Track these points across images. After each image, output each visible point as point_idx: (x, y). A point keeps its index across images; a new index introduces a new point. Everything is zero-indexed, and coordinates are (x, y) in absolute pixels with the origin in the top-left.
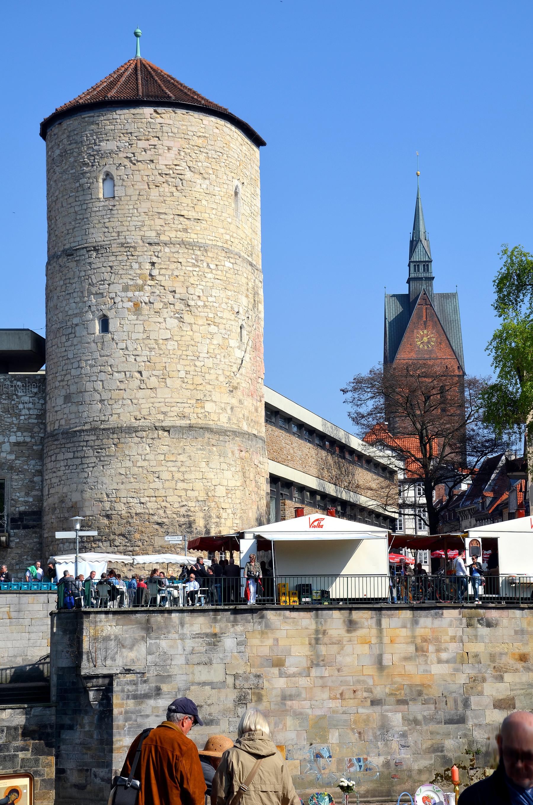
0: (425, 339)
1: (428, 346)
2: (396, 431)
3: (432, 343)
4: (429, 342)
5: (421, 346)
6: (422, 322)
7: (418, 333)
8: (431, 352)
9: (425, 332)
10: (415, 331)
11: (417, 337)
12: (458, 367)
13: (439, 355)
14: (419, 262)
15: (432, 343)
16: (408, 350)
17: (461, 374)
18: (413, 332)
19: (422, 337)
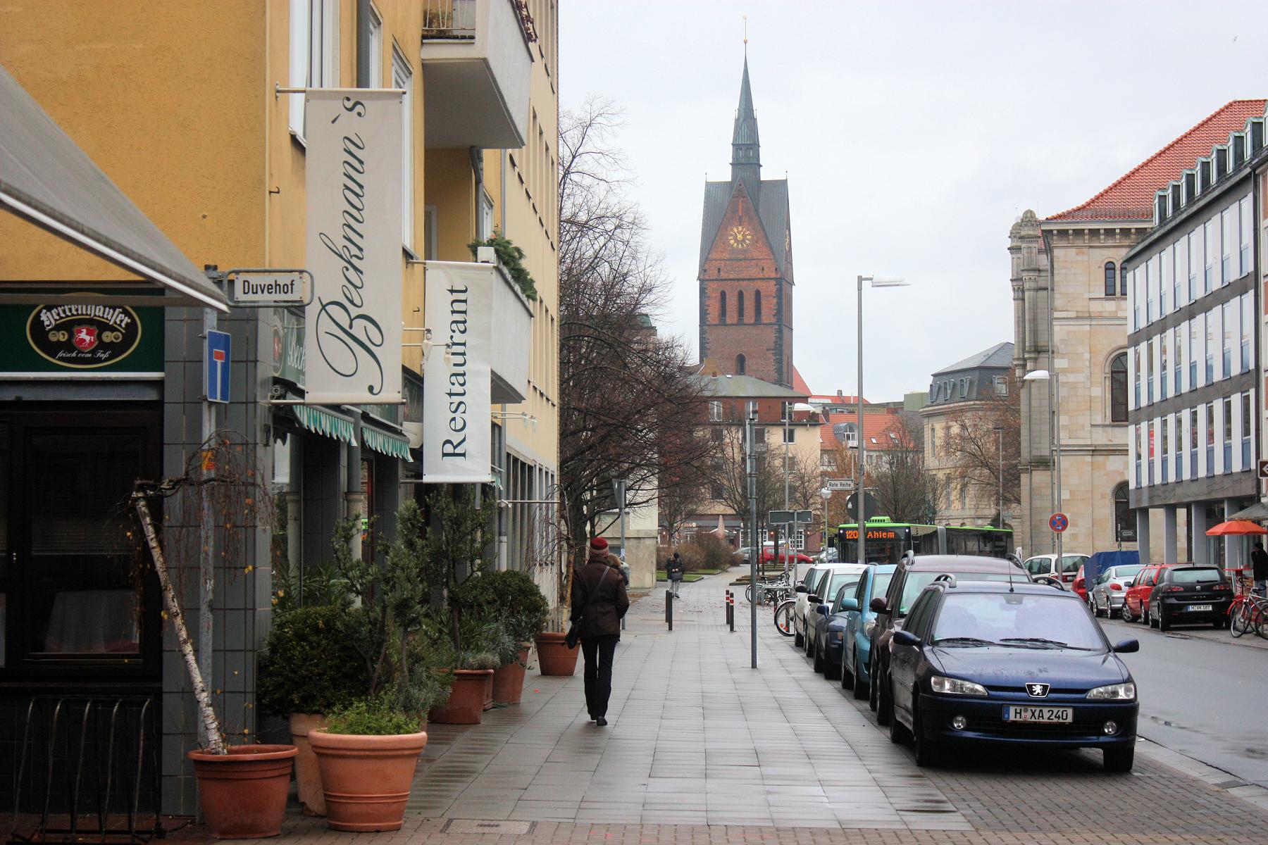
0: (740, 237)
4: (743, 240)
8: (745, 251)
13: (756, 254)
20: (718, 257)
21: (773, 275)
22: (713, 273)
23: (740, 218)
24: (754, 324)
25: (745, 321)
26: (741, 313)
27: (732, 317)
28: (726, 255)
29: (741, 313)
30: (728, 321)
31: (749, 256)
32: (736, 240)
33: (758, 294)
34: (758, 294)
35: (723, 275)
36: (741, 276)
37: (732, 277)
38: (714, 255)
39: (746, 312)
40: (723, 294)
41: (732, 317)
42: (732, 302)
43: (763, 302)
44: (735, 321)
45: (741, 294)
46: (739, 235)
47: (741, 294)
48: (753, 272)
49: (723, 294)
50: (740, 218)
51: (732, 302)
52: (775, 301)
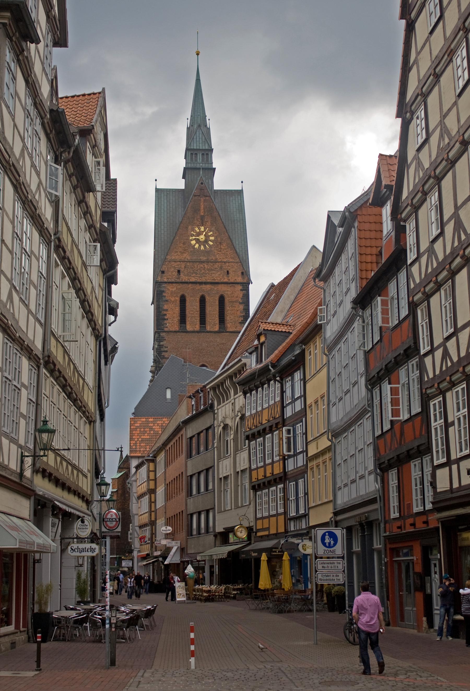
0: (202, 238)
1: (205, 246)
2: (162, 350)
3: (211, 243)
4: (206, 241)
5: (197, 246)
6: (199, 217)
7: (193, 230)
9: (202, 229)
10: (190, 227)
11: (192, 235)
12: (242, 273)
13: (219, 257)
14: (197, 150)
15: (211, 243)
16: (180, 249)
17: (245, 281)
18: (187, 228)
19: (199, 234)
20: (177, 257)
21: (240, 279)
22: (171, 275)
23: (202, 218)
24: (219, 332)
25: (208, 328)
26: (203, 321)
27: (193, 323)
28: (187, 256)
29: (203, 321)
30: (189, 328)
31: (212, 258)
32: (198, 241)
33: (222, 300)
34: (222, 300)
35: (184, 278)
36: (203, 280)
37: (193, 280)
38: (174, 256)
39: (208, 319)
40: (183, 300)
41: (193, 323)
42: (193, 308)
43: (228, 307)
44: (197, 328)
45: (203, 300)
46: (200, 237)
47: (203, 300)
48: (217, 276)
49: (183, 300)
50: (202, 218)
51: (193, 308)
52: (242, 307)
